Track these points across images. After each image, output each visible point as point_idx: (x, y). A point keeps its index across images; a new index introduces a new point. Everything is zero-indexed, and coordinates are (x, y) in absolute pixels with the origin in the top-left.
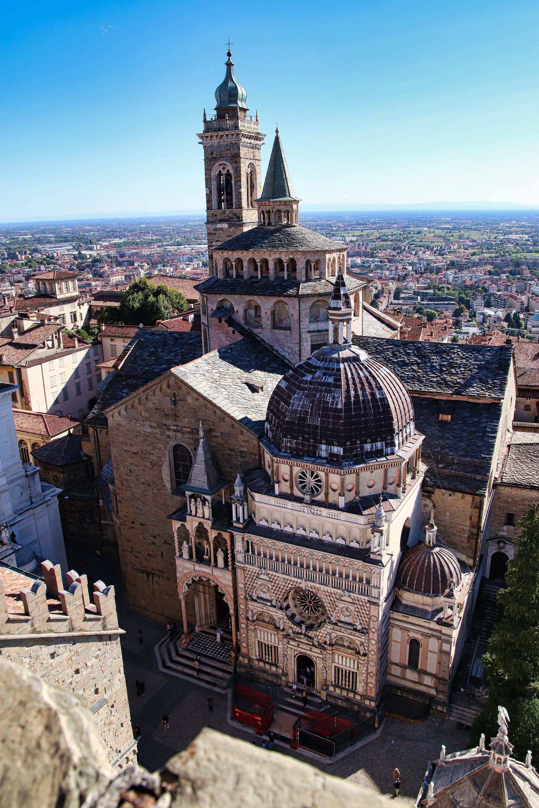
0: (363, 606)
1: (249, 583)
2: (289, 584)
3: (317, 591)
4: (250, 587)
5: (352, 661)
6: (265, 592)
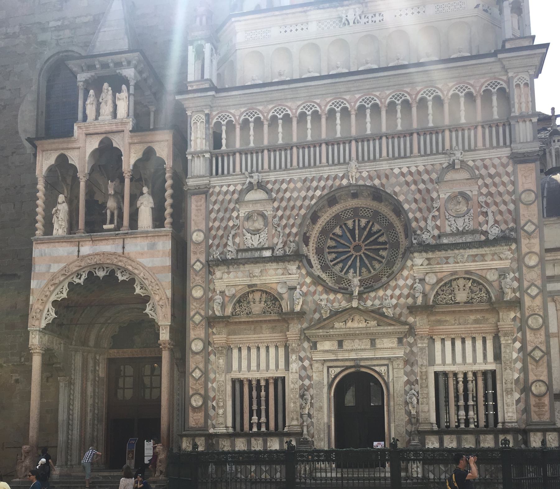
0: (498, 174)
1: (217, 224)
2: (316, 189)
3: (384, 181)
4: (220, 232)
6: (256, 232)
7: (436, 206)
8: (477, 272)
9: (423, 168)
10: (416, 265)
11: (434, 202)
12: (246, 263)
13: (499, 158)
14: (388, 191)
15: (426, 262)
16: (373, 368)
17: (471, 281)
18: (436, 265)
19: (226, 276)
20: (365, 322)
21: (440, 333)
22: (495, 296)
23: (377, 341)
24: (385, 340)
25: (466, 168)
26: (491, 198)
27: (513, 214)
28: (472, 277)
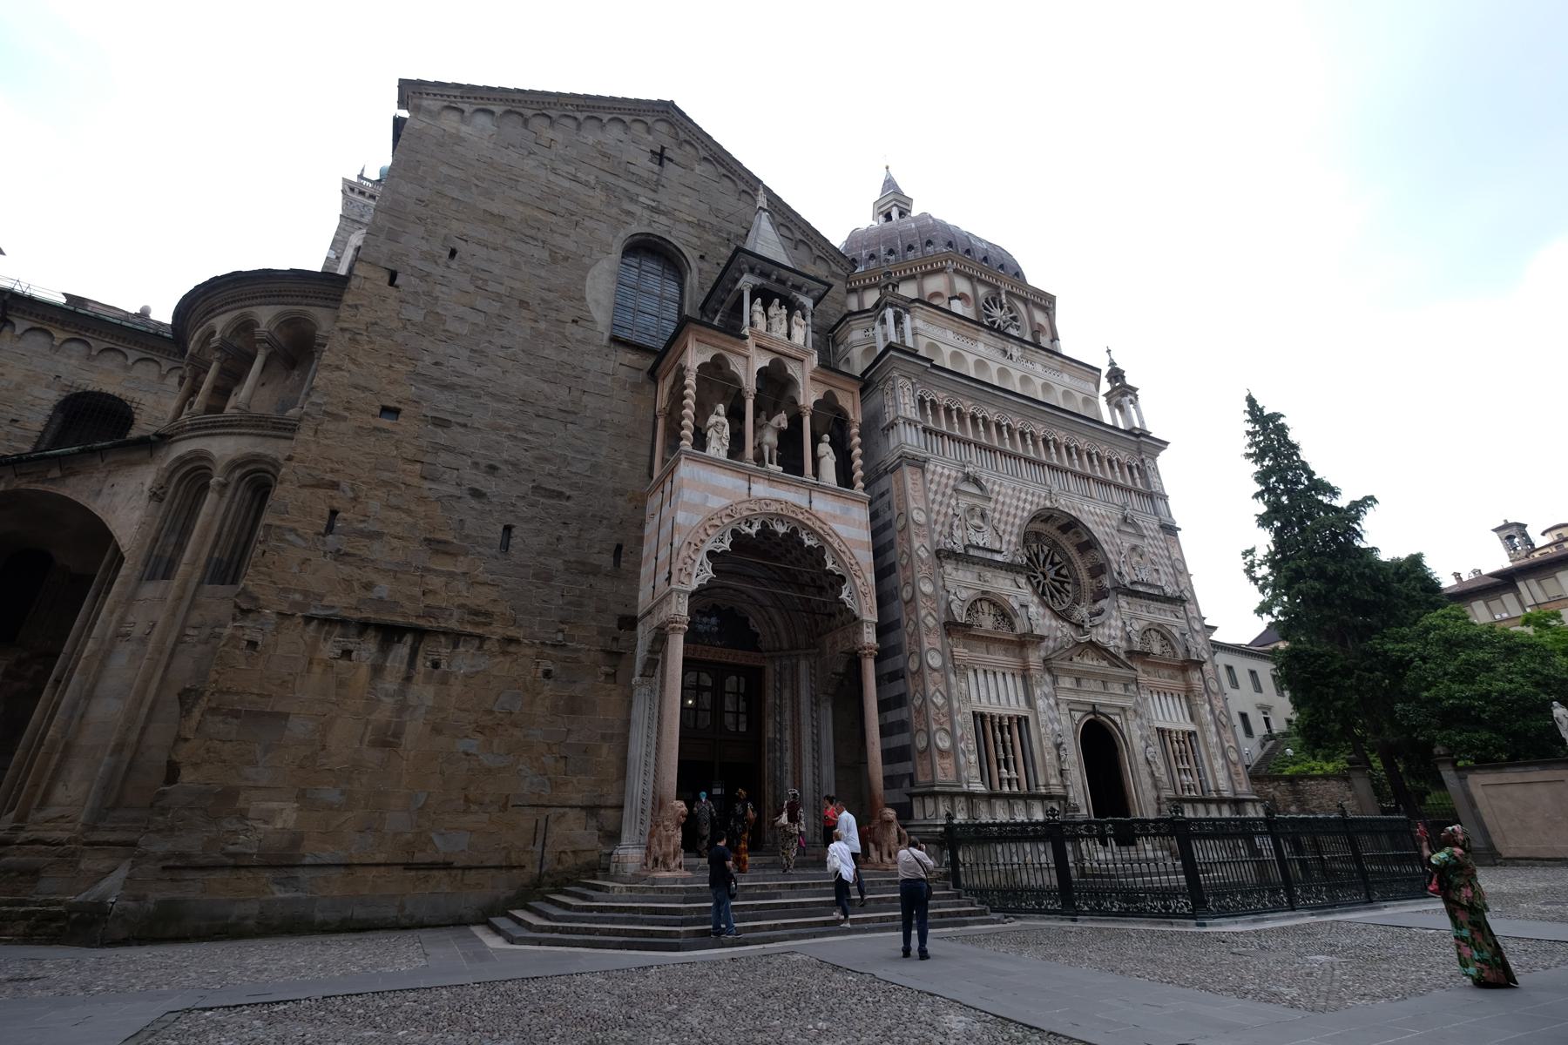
3: (1078, 513)
4: (941, 519)
5: (1176, 700)
12: (978, 564)
19: (954, 573)
24: (1115, 685)
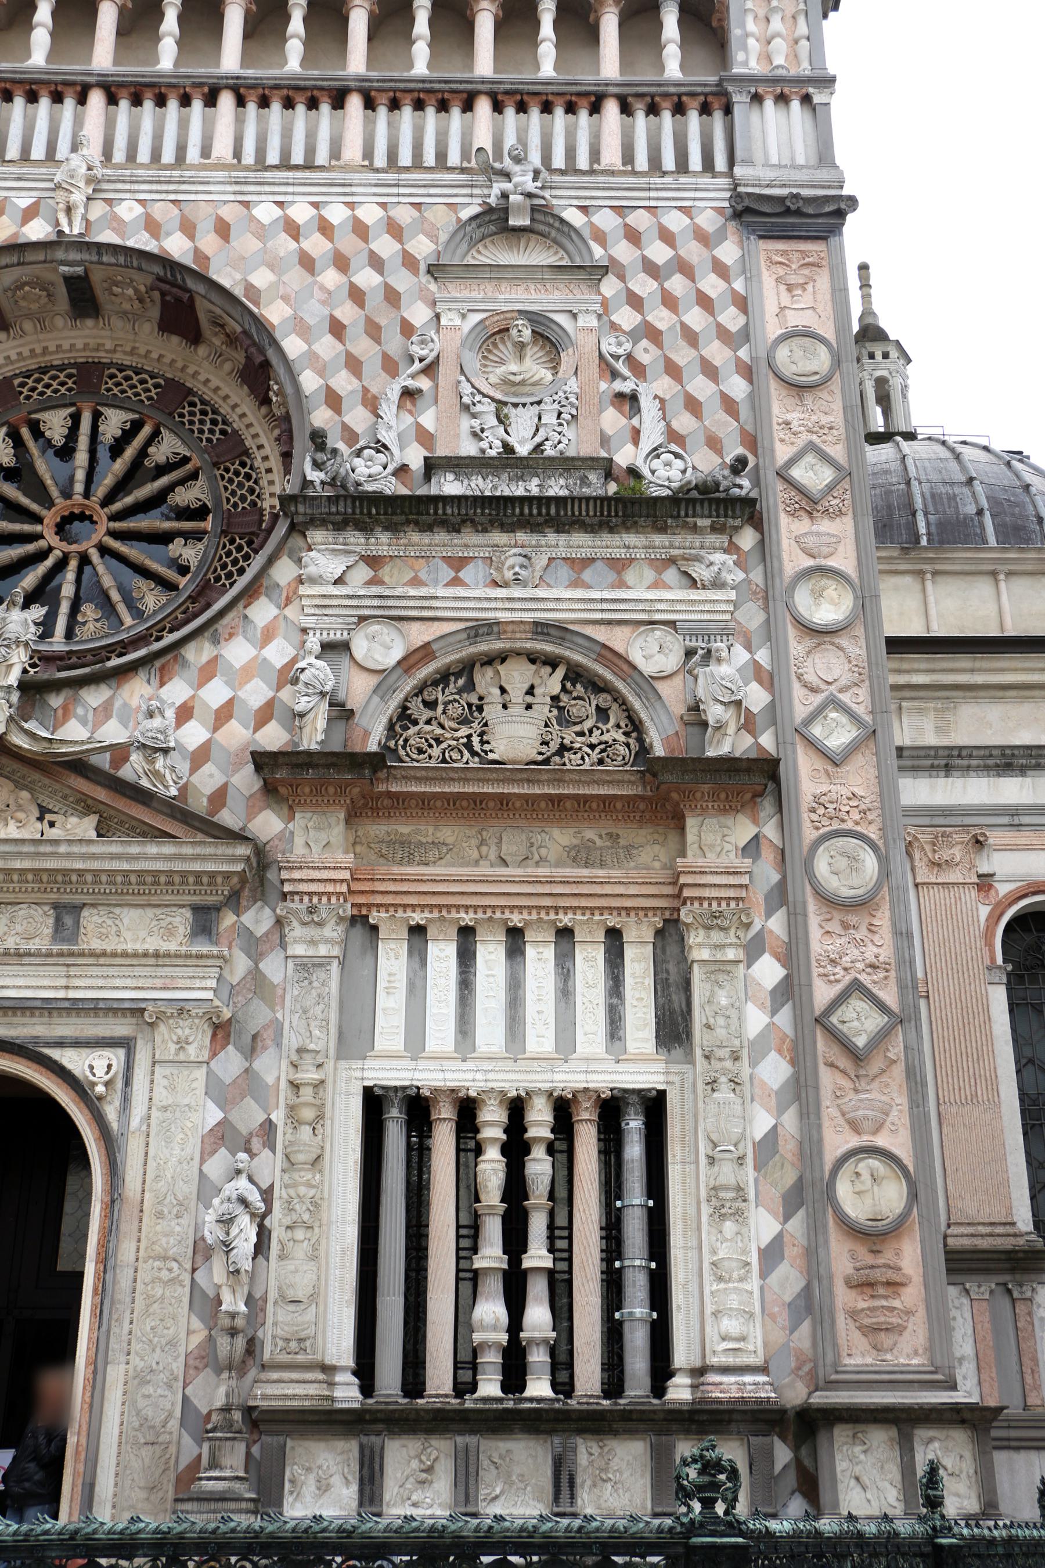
0: (685, 269)
3: (208, 243)
7: (424, 353)
8: (588, 631)
9: (379, 213)
10: (313, 581)
11: (414, 339)
13: (686, 211)
14: (226, 282)
15: (364, 572)
16: (47, 1051)
17: (560, 672)
18: (405, 584)
20: (41, 819)
21: (398, 900)
22: (666, 741)
23: (90, 919)
24: (129, 916)
25: (553, 233)
26: (652, 348)
27: (744, 412)
28: (567, 653)
